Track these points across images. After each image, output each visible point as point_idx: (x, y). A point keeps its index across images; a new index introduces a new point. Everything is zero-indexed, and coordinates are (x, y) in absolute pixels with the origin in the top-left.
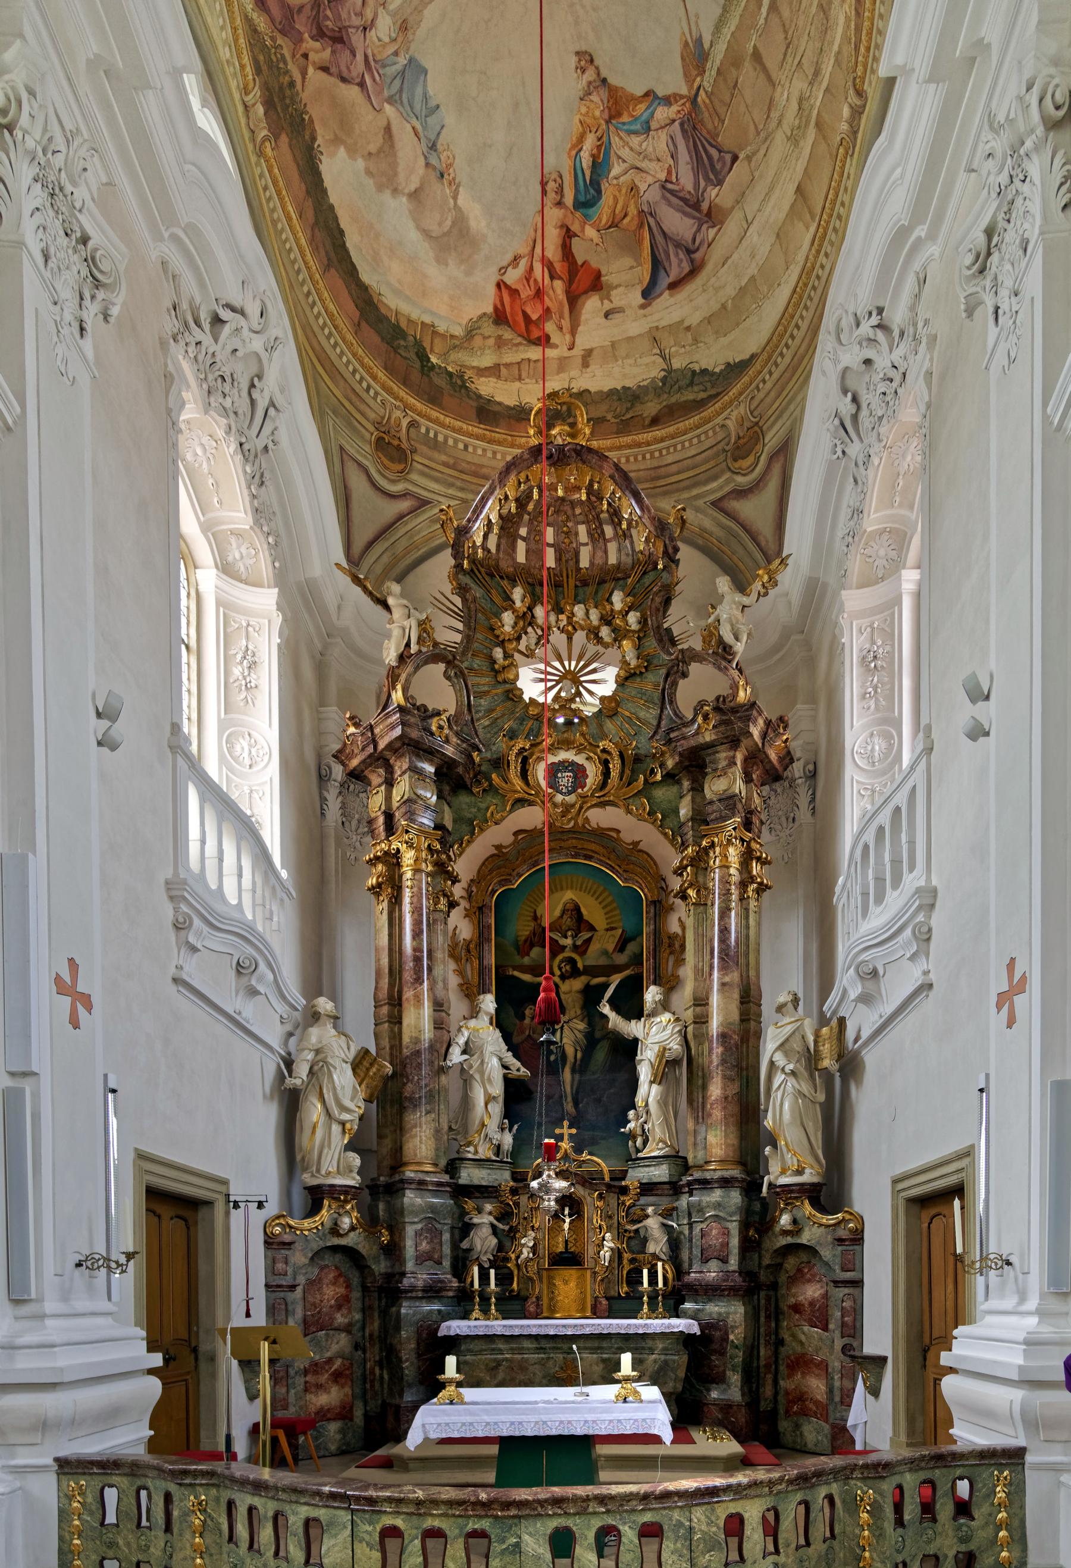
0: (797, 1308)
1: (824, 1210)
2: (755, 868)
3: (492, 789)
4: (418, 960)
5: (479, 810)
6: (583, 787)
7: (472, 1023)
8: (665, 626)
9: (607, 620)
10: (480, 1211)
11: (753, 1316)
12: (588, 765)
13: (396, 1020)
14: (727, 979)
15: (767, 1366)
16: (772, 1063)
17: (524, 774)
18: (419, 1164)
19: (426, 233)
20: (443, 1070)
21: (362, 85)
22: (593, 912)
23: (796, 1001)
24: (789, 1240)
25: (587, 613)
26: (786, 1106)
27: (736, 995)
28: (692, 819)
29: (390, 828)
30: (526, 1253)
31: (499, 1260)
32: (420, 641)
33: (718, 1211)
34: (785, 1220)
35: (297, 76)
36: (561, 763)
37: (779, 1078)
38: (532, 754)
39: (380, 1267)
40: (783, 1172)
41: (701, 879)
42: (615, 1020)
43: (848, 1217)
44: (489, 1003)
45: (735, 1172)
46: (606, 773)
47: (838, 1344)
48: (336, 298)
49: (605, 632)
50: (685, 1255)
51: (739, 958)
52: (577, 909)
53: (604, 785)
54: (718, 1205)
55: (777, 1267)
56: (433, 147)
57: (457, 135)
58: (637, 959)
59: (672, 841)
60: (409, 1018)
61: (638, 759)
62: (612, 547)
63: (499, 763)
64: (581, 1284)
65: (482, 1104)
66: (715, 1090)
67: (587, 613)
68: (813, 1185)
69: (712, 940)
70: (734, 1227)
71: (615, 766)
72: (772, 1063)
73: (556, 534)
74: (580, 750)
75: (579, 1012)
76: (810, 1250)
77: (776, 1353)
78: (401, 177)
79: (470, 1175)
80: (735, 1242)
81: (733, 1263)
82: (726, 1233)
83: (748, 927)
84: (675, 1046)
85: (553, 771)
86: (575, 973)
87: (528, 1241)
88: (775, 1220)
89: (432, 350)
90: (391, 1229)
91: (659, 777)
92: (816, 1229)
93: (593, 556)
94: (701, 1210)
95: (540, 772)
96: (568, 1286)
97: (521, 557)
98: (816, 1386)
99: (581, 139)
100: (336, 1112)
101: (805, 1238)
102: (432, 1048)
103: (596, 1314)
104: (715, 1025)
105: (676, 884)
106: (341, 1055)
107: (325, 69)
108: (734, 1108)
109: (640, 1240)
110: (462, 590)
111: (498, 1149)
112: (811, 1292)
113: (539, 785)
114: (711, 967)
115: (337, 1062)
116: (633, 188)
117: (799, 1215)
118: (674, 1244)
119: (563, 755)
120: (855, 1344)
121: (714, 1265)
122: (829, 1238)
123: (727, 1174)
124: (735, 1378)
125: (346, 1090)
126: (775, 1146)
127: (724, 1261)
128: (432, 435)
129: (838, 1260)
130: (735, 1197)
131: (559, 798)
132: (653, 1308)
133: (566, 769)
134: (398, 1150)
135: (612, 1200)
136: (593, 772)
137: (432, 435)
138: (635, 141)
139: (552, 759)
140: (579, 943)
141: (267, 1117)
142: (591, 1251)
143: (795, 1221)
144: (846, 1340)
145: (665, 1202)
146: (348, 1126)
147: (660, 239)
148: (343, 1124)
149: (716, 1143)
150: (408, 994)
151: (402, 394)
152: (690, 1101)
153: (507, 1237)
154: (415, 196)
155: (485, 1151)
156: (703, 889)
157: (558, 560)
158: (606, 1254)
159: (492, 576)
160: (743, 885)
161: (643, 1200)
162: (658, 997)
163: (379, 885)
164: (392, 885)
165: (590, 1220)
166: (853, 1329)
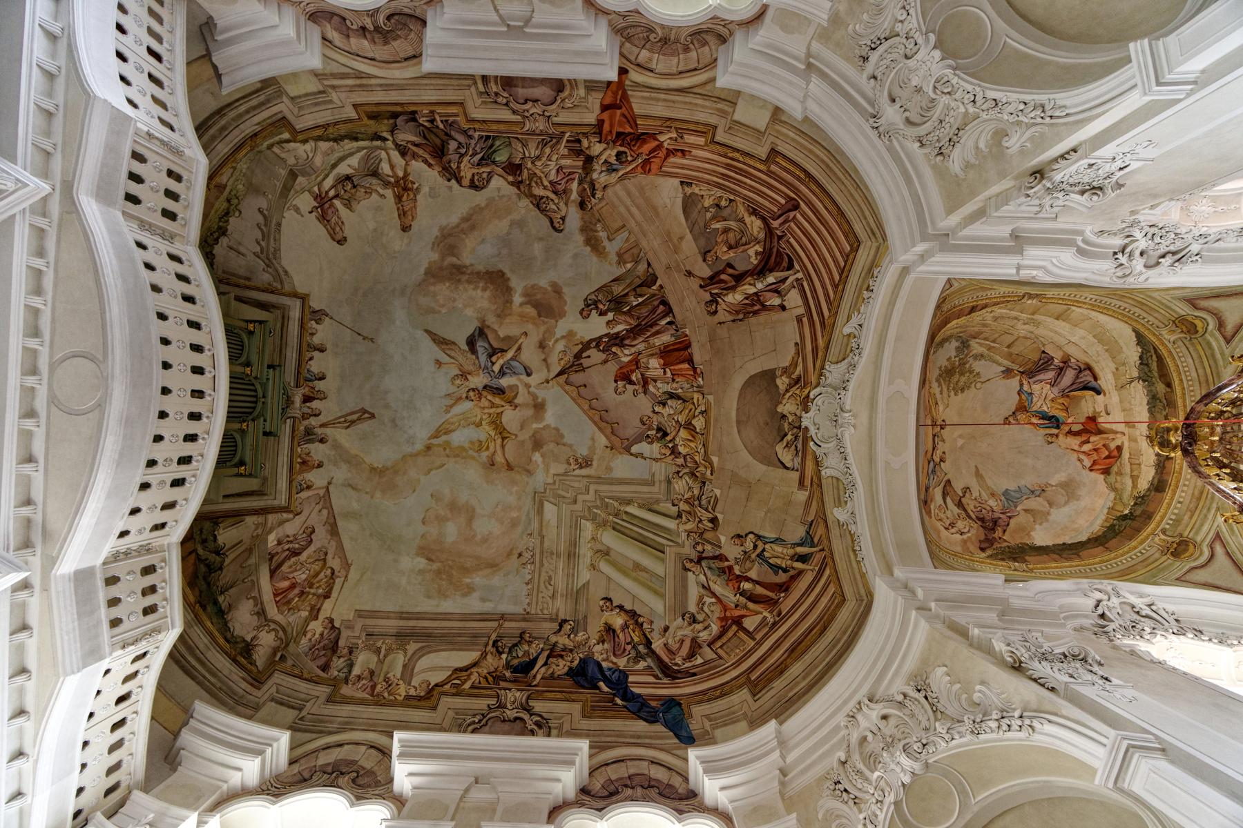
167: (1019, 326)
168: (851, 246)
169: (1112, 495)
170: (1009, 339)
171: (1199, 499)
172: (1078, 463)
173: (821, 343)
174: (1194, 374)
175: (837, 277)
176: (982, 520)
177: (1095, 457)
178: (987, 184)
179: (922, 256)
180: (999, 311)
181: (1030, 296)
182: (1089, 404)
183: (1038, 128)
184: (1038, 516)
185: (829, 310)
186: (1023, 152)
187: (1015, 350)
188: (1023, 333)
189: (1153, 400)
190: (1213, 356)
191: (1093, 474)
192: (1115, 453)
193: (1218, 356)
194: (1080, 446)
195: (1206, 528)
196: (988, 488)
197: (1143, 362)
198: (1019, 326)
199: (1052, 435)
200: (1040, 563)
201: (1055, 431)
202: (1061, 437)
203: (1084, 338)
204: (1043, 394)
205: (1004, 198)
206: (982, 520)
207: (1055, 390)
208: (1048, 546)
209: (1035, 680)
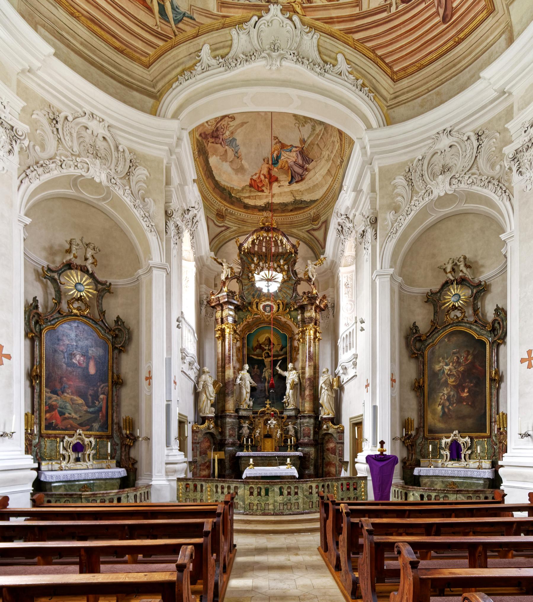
0: (328, 449)
1: (335, 424)
2: (318, 335)
3: (248, 310)
4: (229, 357)
7: (242, 372)
10: (245, 423)
11: (317, 452)
15: (321, 465)
19: (233, 169)
20: (235, 385)
21: (221, 144)
24: (326, 432)
26: (325, 397)
27: (313, 368)
29: (222, 322)
30: (257, 434)
31: (249, 436)
32: (231, 274)
33: (308, 423)
34: (325, 427)
35: (206, 145)
36: (267, 305)
39: (219, 437)
40: (324, 414)
42: (280, 371)
44: (247, 367)
46: (279, 308)
47: (338, 459)
48: (209, 184)
50: (299, 435)
51: (313, 358)
53: (278, 310)
54: (308, 422)
55: (323, 439)
56: (237, 152)
57: (243, 151)
59: (296, 326)
61: (287, 304)
62: (280, 248)
63: (250, 304)
64: (272, 443)
66: (307, 392)
70: (312, 428)
72: (321, 387)
73: (266, 244)
74: (272, 302)
76: (331, 434)
77: (323, 461)
78: (228, 159)
79: (242, 413)
80: (312, 432)
81: (312, 437)
82: (310, 430)
84: (296, 380)
85: (265, 307)
86: (269, 356)
87: (258, 431)
88: (322, 427)
90: (221, 427)
92: (333, 429)
93: (275, 249)
94: (303, 424)
95: (261, 307)
96: (268, 443)
97: (256, 249)
98: (333, 470)
101: (330, 431)
102: (233, 380)
103: (276, 451)
104: (307, 375)
105: (297, 337)
107: (213, 143)
108: (312, 397)
109: (287, 431)
111: (249, 406)
112: (331, 445)
114: (306, 361)
118: (296, 432)
119: (267, 303)
123: (310, 414)
126: (322, 407)
127: (309, 437)
130: (312, 421)
131: (266, 314)
132: (291, 449)
134: (224, 406)
135: (280, 421)
136: (275, 308)
138: (288, 153)
139: (264, 304)
142: (274, 434)
143: (327, 427)
147: (294, 172)
149: (308, 406)
150: (227, 366)
152: (301, 394)
153: (252, 430)
154: (231, 162)
155: (246, 407)
156: (304, 339)
157: (266, 250)
158: (278, 435)
160: (315, 339)
161: (288, 420)
163: (219, 337)
164: (223, 336)
166: (342, 455)
167: (328, 152)
168: (395, 73)
169: (240, 189)
170: (322, 146)
171: (243, 221)
172: (254, 173)
173: (336, 28)
174: (295, 220)
175: (379, 53)
176: (217, 130)
177: (258, 181)
178: (382, 197)
179: (365, 148)
180: (337, 146)
181: (342, 162)
182: (284, 179)
183: (389, 229)
184: (224, 157)
185: (358, 40)
186: (385, 219)
187: (315, 147)
188: (324, 153)
189: (285, 205)
190: (302, 226)
191: (249, 180)
192: (260, 189)
193: (302, 228)
194: (263, 174)
195: (232, 224)
196: (236, 130)
197: (302, 202)
198: (328, 152)
199: (268, 161)
200: (200, 163)
201: (270, 162)
202: (268, 165)
203: (317, 179)
204: (290, 158)
205: (373, 202)
206: (217, 130)
207: (292, 163)
208: (209, 164)
209: (166, 224)
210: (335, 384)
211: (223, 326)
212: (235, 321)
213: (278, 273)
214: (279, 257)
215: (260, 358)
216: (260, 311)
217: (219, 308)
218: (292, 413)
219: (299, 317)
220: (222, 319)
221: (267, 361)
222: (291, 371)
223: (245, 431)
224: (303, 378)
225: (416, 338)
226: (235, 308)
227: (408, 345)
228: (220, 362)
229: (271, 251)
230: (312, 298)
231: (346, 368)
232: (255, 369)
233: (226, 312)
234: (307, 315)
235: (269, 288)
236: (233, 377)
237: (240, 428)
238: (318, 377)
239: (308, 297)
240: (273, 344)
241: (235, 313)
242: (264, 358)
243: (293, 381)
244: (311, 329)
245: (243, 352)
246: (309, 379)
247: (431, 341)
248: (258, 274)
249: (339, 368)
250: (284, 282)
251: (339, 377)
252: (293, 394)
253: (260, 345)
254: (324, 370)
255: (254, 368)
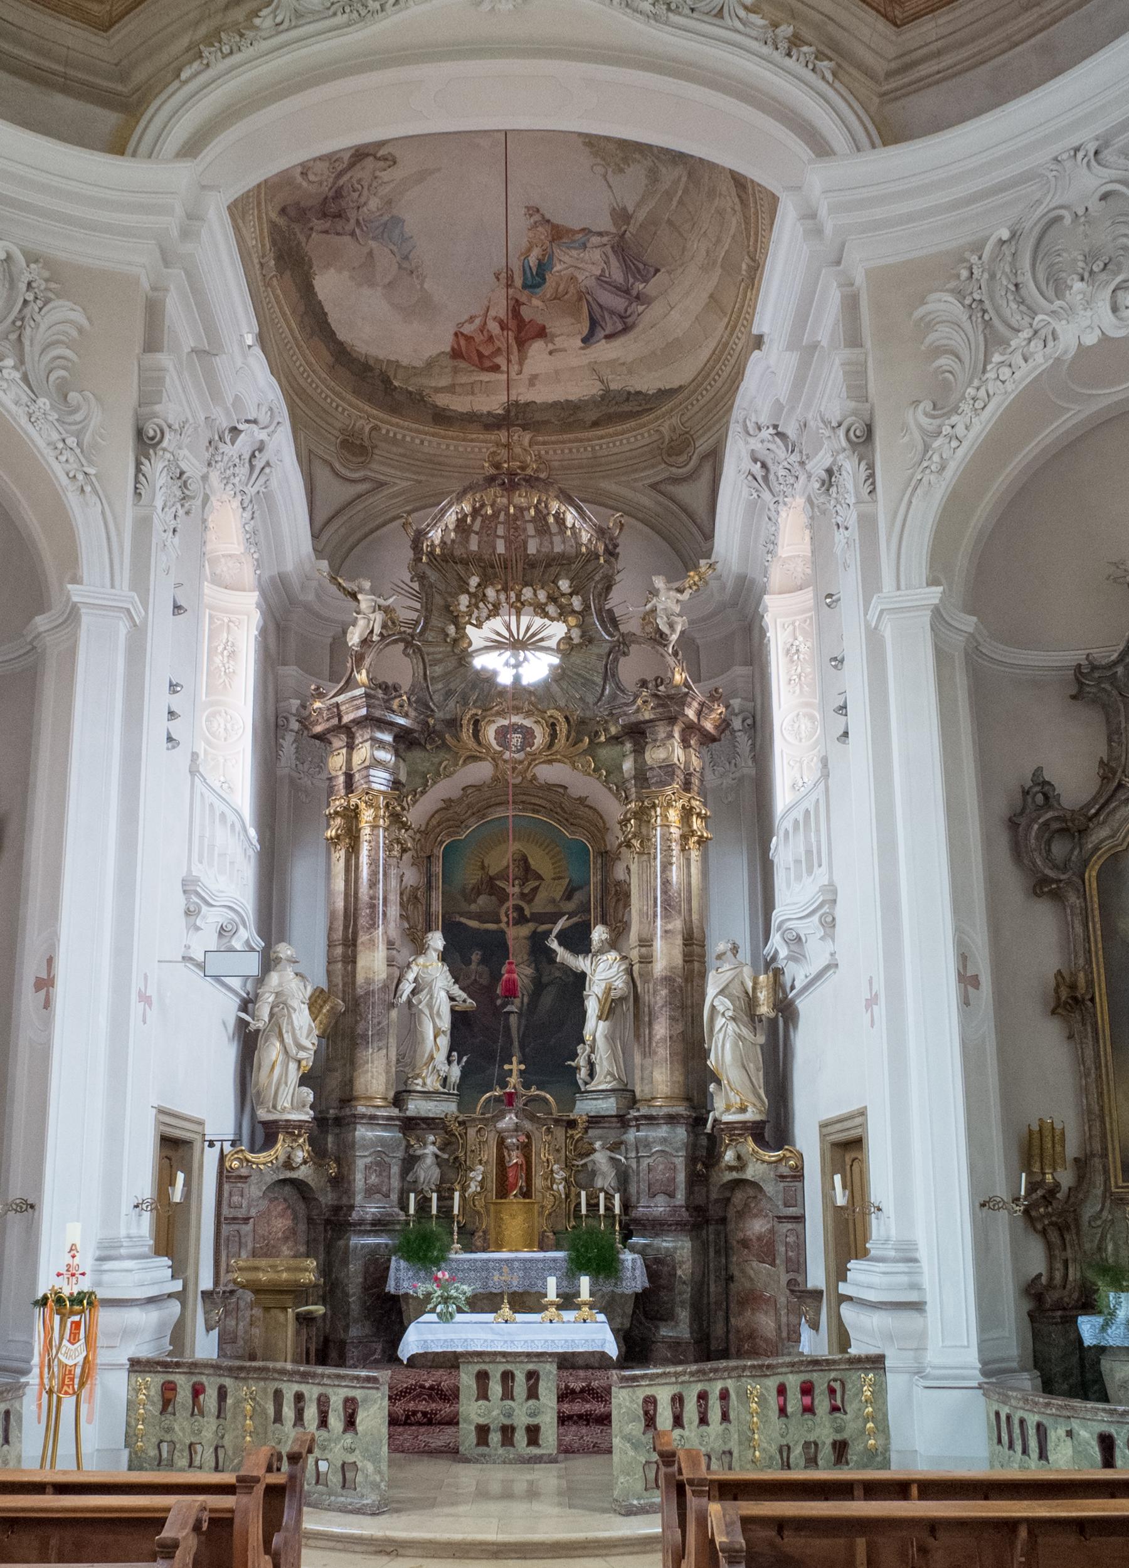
2: (696, 824)
3: (444, 746)
4: (373, 907)
5: (433, 764)
6: (531, 747)
8: (607, 607)
9: (552, 599)
12: (535, 727)
13: (351, 960)
14: (670, 927)
16: (713, 1007)
17: (476, 734)
18: (371, 1098)
22: (540, 862)
23: (735, 949)
25: (535, 594)
27: (679, 941)
28: (635, 777)
29: (349, 786)
37: (720, 1022)
38: (485, 717)
41: (644, 831)
43: (788, 1154)
45: (681, 1109)
46: (553, 735)
49: (552, 609)
52: (525, 859)
53: (551, 745)
58: (585, 908)
59: (617, 795)
60: (362, 962)
61: (582, 722)
63: (453, 724)
65: (432, 1038)
67: (535, 594)
68: (754, 1122)
69: (655, 890)
71: (562, 728)
72: (713, 1007)
74: (529, 714)
75: (526, 957)
83: (689, 875)
84: (620, 984)
89: (395, 377)
91: (603, 739)
95: (490, 733)
99: (529, 250)
100: (293, 1050)
102: (385, 987)
104: (660, 967)
106: (298, 993)
110: (421, 578)
113: (490, 744)
114: (655, 916)
115: (295, 1003)
116: (573, 278)
117: (743, 1152)
120: (799, 1279)
121: (661, 1199)
122: (772, 1175)
124: (684, 1315)
125: (303, 1027)
128: (391, 435)
129: (781, 1196)
133: (515, 731)
137: (391, 435)
138: (574, 253)
140: (526, 891)
141: (229, 1054)
144: (792, 1275)
145: (612, 1136)
146: (304, 1063)
148: (299, 1062)
149: (660, 1080)
150: (363, 938)
151: (366, 407)
156: (645, 840)
159: (447, 562)
160: (684, 838)
162: (605, 936)
163: (338, 837)
164: (352, 836)
165: (538, 1154)
210: (762, 996)
211: (354, 800)
212: (396, 784)
213: (552, 619)
214: (554, 570)
215: (491, 926)
216: (488, 747)
217: (339, 742)
218: (608, 1106)
219: (628, 765)
220: (349, 777)
221: (517, 935)
222: (601, 951)
223: (428, 1172)
224: (646, 976)
225: (1046, 824)
226: (396, 738)
227: (1018, 850)
228: (339, 924)
229: (526, 549)
230: (670, 697)
231: (798, 939)
232: (473, 966)
233: (363, 753)
234: (654, 756)
235: (521, 670)
236: (384, 976)
237: (410, 1162)
238: (703, 975)
239: (655, 696)
240: (539, 877)
241: (397, 754)
242: (503, 925)
243: (609, 990)
244: (669, 805)
245: (429, 905)
246: (668, 980)
247: (1104, 832)
248: (479, 626)
249: (776, 939)
250: (567, 648)
251: (778, 973)
252: (610, 1038)
253: (491, 879)
254: (722, 947)
255: (468, 962)
